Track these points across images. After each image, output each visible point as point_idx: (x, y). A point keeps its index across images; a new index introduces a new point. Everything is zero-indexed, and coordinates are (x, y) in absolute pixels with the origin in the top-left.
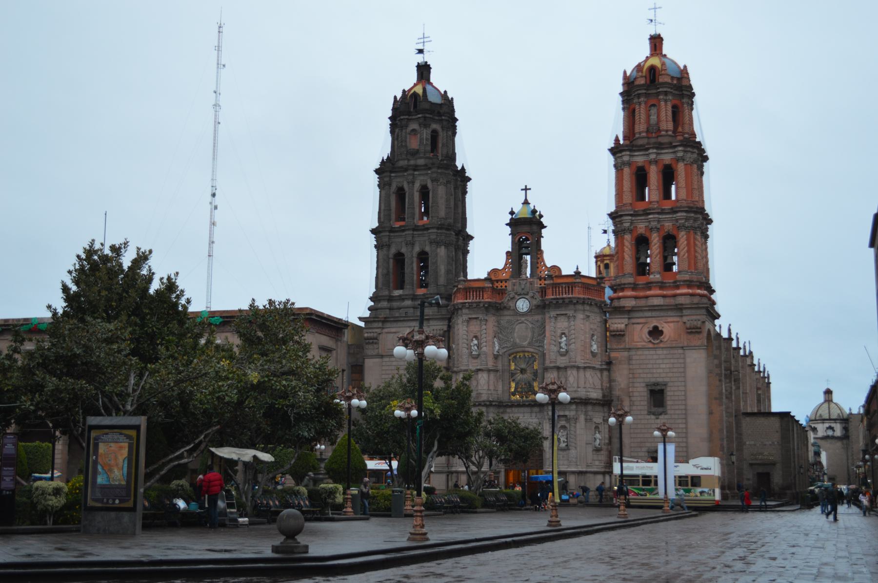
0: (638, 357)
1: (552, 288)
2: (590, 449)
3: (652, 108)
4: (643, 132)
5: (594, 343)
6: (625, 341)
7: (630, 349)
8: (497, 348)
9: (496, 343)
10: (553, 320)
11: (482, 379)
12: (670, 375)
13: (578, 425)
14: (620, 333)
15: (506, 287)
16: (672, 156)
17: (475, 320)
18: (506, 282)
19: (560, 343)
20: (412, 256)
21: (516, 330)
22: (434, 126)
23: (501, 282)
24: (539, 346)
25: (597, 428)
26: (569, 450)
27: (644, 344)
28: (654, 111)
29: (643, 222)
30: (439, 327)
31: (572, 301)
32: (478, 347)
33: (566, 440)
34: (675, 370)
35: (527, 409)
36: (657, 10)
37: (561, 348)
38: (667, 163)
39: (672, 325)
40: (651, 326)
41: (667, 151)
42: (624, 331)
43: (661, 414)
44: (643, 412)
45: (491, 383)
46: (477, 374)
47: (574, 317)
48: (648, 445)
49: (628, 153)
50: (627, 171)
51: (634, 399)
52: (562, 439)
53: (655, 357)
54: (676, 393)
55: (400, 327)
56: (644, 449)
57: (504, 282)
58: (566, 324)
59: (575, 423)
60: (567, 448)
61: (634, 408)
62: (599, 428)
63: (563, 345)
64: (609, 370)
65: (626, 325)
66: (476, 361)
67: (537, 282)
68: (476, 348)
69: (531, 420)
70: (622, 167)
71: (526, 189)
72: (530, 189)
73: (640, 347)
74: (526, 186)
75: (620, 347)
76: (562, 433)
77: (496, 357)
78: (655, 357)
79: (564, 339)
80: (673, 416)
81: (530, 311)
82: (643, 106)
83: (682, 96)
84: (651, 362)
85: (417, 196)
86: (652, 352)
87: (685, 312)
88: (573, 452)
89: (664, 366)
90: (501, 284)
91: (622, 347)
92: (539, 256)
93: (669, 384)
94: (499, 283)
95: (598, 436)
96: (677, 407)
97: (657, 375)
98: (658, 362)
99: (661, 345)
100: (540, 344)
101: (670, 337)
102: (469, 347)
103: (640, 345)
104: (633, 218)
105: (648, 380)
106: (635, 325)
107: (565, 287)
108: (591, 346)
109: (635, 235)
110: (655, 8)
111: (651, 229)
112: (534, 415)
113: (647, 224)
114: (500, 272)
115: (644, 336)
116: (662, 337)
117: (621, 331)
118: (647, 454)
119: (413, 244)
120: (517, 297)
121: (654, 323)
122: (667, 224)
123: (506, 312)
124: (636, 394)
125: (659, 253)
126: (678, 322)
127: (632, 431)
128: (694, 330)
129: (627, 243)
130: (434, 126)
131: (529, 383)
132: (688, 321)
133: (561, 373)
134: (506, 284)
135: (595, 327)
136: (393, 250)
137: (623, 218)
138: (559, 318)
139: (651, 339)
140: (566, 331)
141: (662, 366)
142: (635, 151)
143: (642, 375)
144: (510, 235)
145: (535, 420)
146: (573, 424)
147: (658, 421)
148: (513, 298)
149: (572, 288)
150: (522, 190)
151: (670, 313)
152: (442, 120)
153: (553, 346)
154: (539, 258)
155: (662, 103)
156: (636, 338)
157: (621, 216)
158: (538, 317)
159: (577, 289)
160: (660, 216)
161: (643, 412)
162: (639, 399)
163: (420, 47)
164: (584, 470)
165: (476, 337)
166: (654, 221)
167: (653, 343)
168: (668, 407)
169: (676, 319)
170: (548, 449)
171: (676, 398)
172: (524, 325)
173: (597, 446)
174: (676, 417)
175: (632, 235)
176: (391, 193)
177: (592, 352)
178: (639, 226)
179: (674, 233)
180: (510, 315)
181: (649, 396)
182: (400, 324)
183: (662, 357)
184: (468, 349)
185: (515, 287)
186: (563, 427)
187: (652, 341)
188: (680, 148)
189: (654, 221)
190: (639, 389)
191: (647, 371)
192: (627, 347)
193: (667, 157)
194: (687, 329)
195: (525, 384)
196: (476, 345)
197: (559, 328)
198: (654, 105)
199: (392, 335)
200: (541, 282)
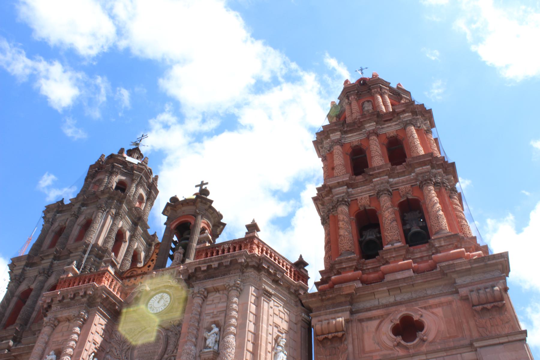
5: (280, 348)
14: (336, 334)
19: (206, 339)
27: (390, 352)
29: (366, 191)
37: (206, 347)
38: (392, 135)
39: (439, 311)
40: (397, 317)
41: (389, 124)
50: (337, 149)
63: (210, 342)
71: (202, 184)
74: (202, 182)
79: (216, 330)
99: (424, 349)
104: (350, 190)
106: (363, 323)
109: (355, 208)
110: (362, 70)
111: (378, 193)
115: (384, 338)
116: (423, 333)
117: (337, 331)
119: (48, 276)
121: (403, 311)
122: (403, 187)
125: (395, 220)
126: (450, 303)
128: (489, 306)
129: (341, 217)
132: (472, 291)
136: (23, 287)
138: (210, 298)
139: (399, 339)
142: (346, 132)
153: (189, 343)
160: (391, 180)
167: (407, 348)
169: (443, 299)
175: (349, 209)
178: (359, 198)
188: (407, 114)
189: (382, 183)
194: (473, 306)
197: (208, 314)
198: (368, 101)
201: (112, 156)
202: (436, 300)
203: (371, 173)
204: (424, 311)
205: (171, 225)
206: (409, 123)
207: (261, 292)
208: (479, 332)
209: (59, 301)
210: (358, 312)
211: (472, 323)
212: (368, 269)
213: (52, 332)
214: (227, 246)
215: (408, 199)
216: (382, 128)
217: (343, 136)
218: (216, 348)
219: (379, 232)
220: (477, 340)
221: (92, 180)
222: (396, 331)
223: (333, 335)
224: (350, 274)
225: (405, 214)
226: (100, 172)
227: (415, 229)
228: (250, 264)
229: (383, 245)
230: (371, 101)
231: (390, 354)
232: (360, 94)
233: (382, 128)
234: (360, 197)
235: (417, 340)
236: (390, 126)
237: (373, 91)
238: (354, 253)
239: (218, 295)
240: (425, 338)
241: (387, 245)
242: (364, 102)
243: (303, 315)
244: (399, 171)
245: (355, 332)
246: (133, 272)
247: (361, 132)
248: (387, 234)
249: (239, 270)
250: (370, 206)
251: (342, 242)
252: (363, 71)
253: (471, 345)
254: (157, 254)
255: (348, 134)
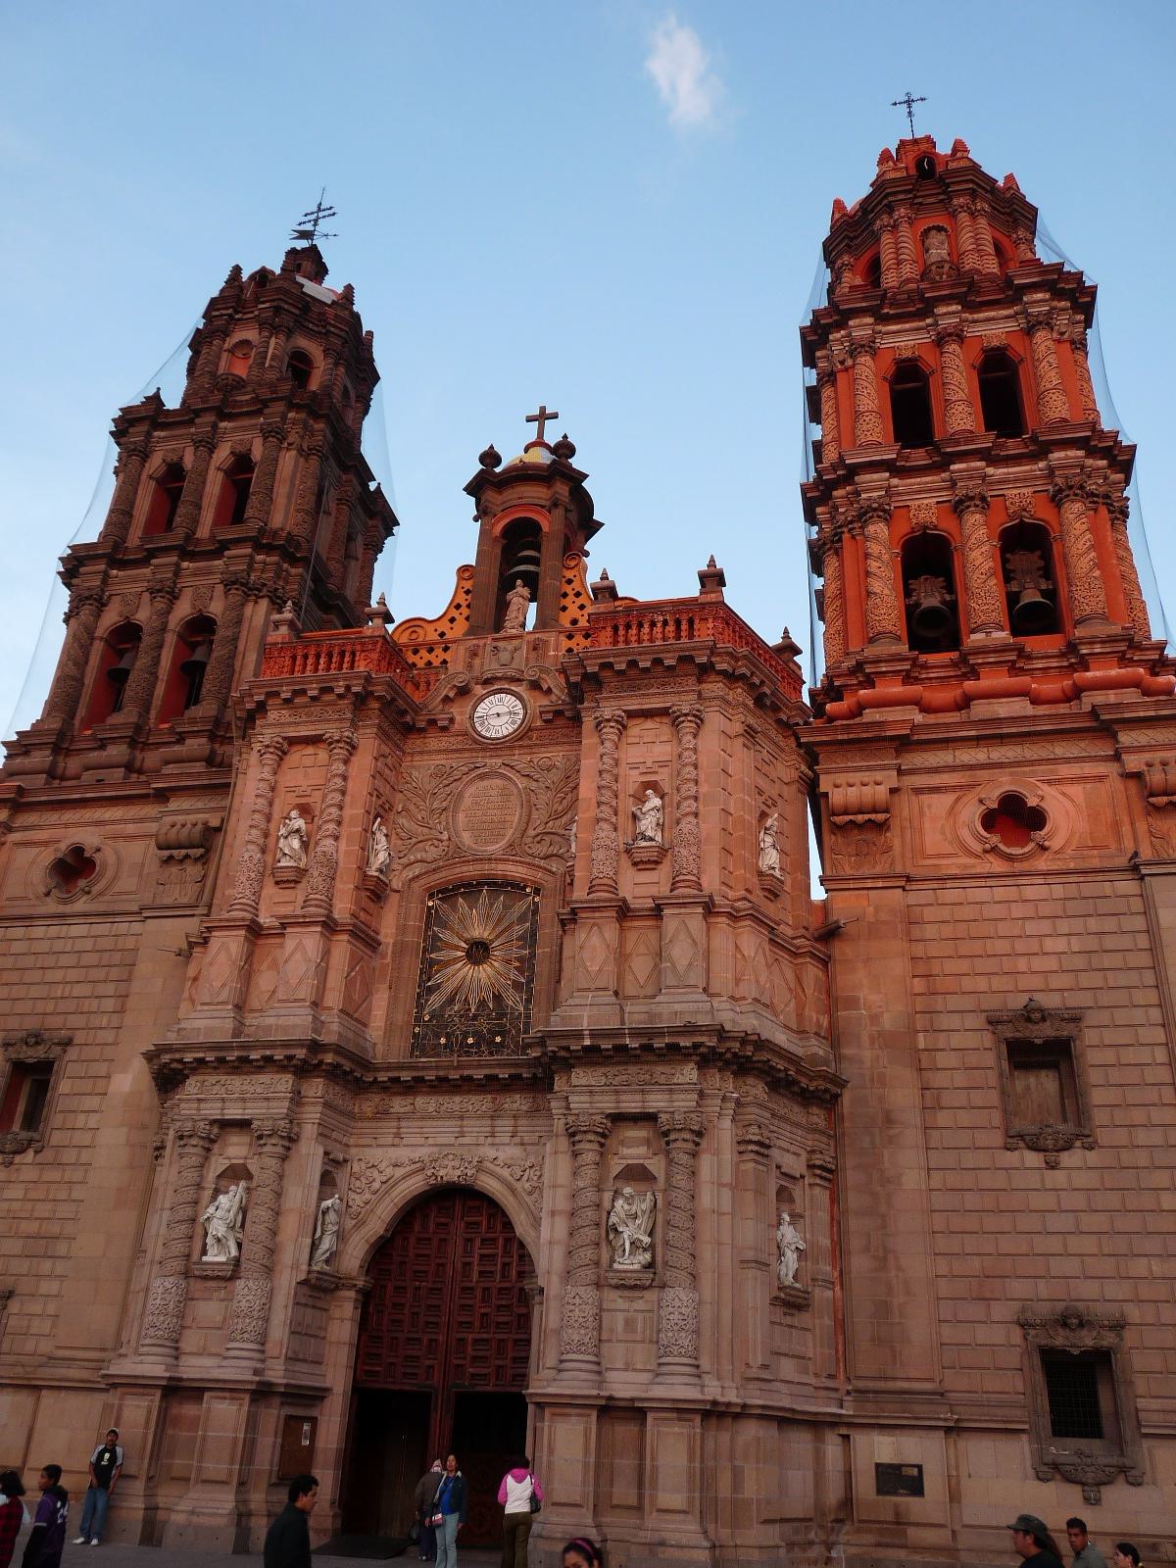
0: (945, 913)
1: (616, 629)
2: (756, 1295)
3: (934, 232)
4: (908, 281)
5: (769, 840)
6: (890, 849)
7: (908, 879)
8: (382, 856)
9: (381, 837)
10: (610, 732)
11: (298, 956)
12: (1096, 979)
13: (706, 1165)
14: (873, 816)
15: (445, 662)
16: (1012, 326)
17: (310, 750)
18: (446, 649)
19: (635, 817)
20: (164, 629)
21: (467, 801)
22: (303, 343)
23: (430, 651)
24: (545, 858)
25: (784, 1195)
26: (663, 1286)
27: (973, 861)
28: (935, 238)
30: (192, 818)
31: (691, 659)
32: (305, 845)
33: (647, 1240)
34: (1108, 961)
35: (480, 1103)
36: (913, 105)
38: (995, 343)
39: (1075, 790)
40: (993, 797)
41: (992, 314)
42: (887, 811)
43: (1068, 1147)
44: (982, 1138)
45: (336, 980)
46: (281, 946)
47: (699, 720)
48: (1019, 1288)
49: (870, 320)
51: (939, 1079)
52: (628, 1233)
53: (1018, 911)
54: (1129, 1055)
55: (66, 826)
56: (1002, 1311)
57: (438, 651)
58: (663, 750)
59: (694, 1155)
60: (652, 1278)
61: (943, 1118)
62: (792, 1200)
63: (647, 825)
64: (825, 962)
65: (893, 791)
66: (288, 895)
67: (557, 641)
68: (296, 843)
69: (491, 1153)
70: (849, 362)
71: (543, 417)
72: (555, 416)
73: (954, 871)
74: (543, 409)
75: (866, 871)
76: (629, 1200)
77: (375, 891)
78: (1018, 911)
79: (656, 802)
80: (1126, 1157)
81: (522, 738)
82: (905, 230)
83: (1015, 224)
84: (1004, 929)
85: (214, 485)
86: (1000, 893)
87: (1126, 738)
88: (678, 1299)
89: (1060, 944)
90: (427, 657)
91: (878, 870)
92: (569, 574)
93: (1092, 1018)
94: (423, 653)
95: (788, 1234)
96: (1138, 1116)
97: (1036, 982)
98: (1031, 928)
99: (1042, 863)
100: (549, 852)
101: (1073, 833)
102: (267, 845)
103: (954, 865)
104: (895, 481)
105: (992, 1003)
106: (921, 797)
107: (665, 623)
108: (759, 851)
109: (903, 528)
110: (909, 102)
112: (505, 1125)
113: (945, 495)
114: (430, 628)
115: (965, 834)
116: (1042, 833)
117: (875, 811)
118: (1017, 1336)
119: (173, 596)
120: (479, 690)
123: (434, 742)
124: (942, 1060)
125: (994, 574)
126: (1101, 778)
127: (939, 1222)
129: (874, 548)
130: (303, 343)
131: (498, 998)
132: (1149, 765)
133: (632, 937)
134: (447, 656)
135: (772, 791)
136: (111, 618)
137: (857, 479)
139: (995, 839)
140: (663, 777)
141: (1050, 945)
143: (967, 984)
144: (476, 519)
145: (510, 1152)
146: (684, 1158)
147: (1058, 1177)
148: (464, 692)
149: (691, 622)
150: (529, 419)
151: (1060, 749)
152: (328, 331)
154: (570, 582)
155: (963, 216)
156: (934, 839)
157: (854, 470)
158: (557, 755)
159: (711, 625)
160: (990, 470)
161: (982, 1138)
162: (960, 1079)
163: (309, 227)
164: (732, 1396)
165: (305, 810)
166: (971, 478)
167: (1010, 858)
168: (1100, 1117)
169: (1089, 769)
170: (555, 1279)
171: (1132, 1076)
172: (499, 782)
173: (789, 1280)
174: (1142, 1158)
176: (144, 476)
177: (760, 874)
179: (1044, 513)
180: (447, 751)
181: (1005, 1064)
182: (70, 816)
183: (1046, 909)
184: (263, 851)
185: (477, 662)
186: (637, 1174)
187: (1001, 846)
188: (1040, 296)
190: (956, 1040)
191: (990, 965)
192: (899, 869)
193: (995, 328)
194: (1152, 795)
195: (482, 1004)
196: (298, 831)
198: (940, 229)
199: (35, 851)
200: (571, 644)
201: (262, 276)
202: (1075, 770)
203: (948, 450)
204: (1046, 787)
205: (493, 525)
206: (1040, 323)
207: (739, 728)
208: (1153, 846)
209: (284, 700)
210: (912, 772)
211: (1142, 827)
212: (931, 679)
213: (279, 766)
214: (661, 618)
215: (1022, 521)
216: (975, 321)
217: (879, 328)
218: (659, 838)
219: (950, 587)
220: (1148, 864)
221: (224, 341)
222: (989, 821)
223: (867, 817)
224: (896, 689)
225: (1008, 556)
226: (239, 319)
227: (1030, 596)
228: (718, 667)
229: (963, 630)
230: (946, 231)
231: (973, 866)
232: (921, 204)
233: (975, 321)
234: (917, 503)
235: (1031, 846)
236: (993, 319)
237: (955, 202)
238: (899, 638)
239: (649, 724)
240: (1046, 843)
241: (973, 631)
242: (929, 229)
243: (803, 768)
244: (1011, 452)
245: (906, 813)
246: (417, 629)
247: (921, 324)
248: (977, 607)
249: (694, 678)
250: (936, 528)
251: (877, 612)
252: (913, 105)
253: (1135, 868)
254: (467, 592)
255: (888, 325)
